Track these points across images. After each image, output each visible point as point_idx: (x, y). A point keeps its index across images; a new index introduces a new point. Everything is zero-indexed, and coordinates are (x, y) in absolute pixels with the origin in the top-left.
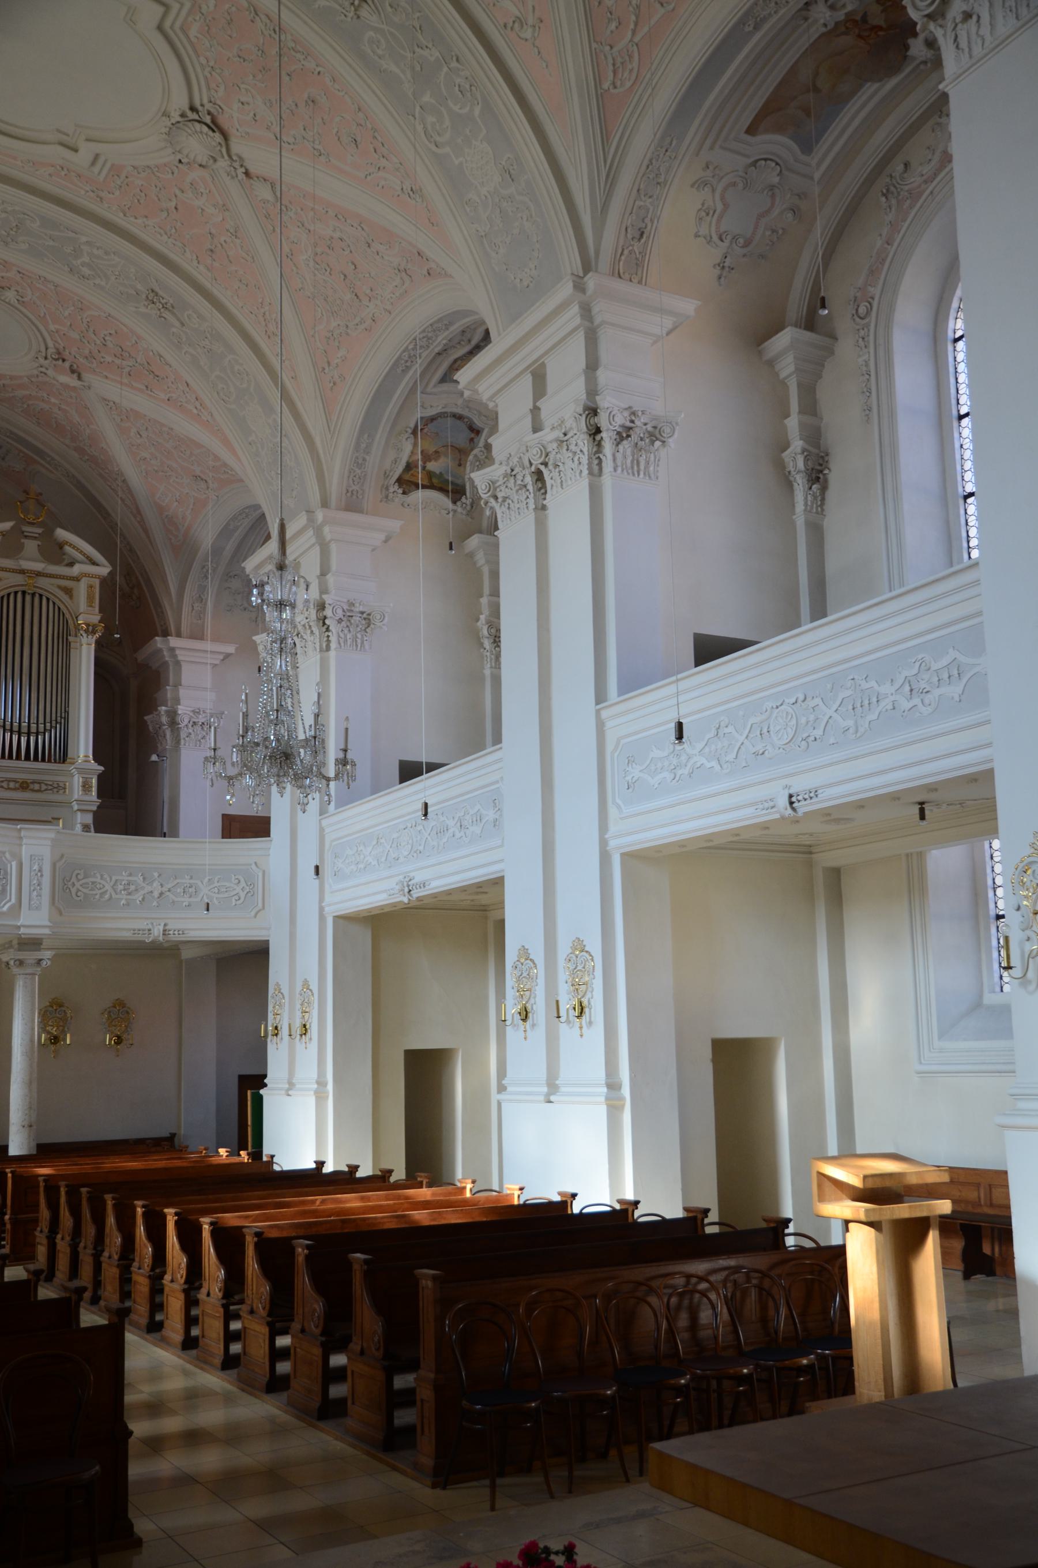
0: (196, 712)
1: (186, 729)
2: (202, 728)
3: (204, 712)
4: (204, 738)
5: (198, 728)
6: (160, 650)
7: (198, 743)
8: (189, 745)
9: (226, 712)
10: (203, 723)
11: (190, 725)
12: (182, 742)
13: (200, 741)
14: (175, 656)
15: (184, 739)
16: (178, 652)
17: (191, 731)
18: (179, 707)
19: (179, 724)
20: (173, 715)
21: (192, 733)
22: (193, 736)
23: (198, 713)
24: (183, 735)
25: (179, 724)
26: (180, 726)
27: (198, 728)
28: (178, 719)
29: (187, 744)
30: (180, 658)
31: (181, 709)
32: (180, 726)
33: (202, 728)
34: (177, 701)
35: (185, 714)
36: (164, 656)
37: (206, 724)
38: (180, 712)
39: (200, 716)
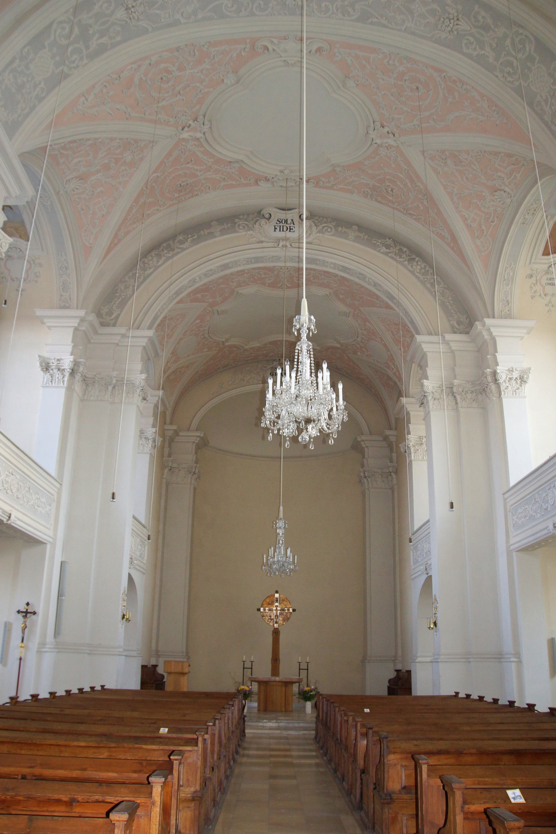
0: (511, 371)
1: (504, 383)
2: (517, 382)
3: (516, 370)
4: (518, 389)
5: (513, 382)
6: (480, 333)
7: (514, 392)
8: (508, 395)
9: (532, 368)
10: (516, 378)
11: (507, 381)
12: (503, 393)
13: (515, 391)
14: (491, 334)
15: (504, 390)
16: (492, 330)
17: (507, 385)
18: (498, 367)
19: (499, 380)
20: (495, 373)
21: (509, 386)
22: (510, 387)
23: (512, 371)
24: (502, 388)
25: (499, 380)
26: (500, 381)
27: (513, 382)
28: (498, 377)
29: (506, 395)
30: (494, 334)
31: (499, 369)
32: (500, 381)
33: (517, 382)
34: (497, 364)
35: (502, 372)
36: (483, 336)
37: (518, 378)
38: (498, 371)
39: (514, 373)
